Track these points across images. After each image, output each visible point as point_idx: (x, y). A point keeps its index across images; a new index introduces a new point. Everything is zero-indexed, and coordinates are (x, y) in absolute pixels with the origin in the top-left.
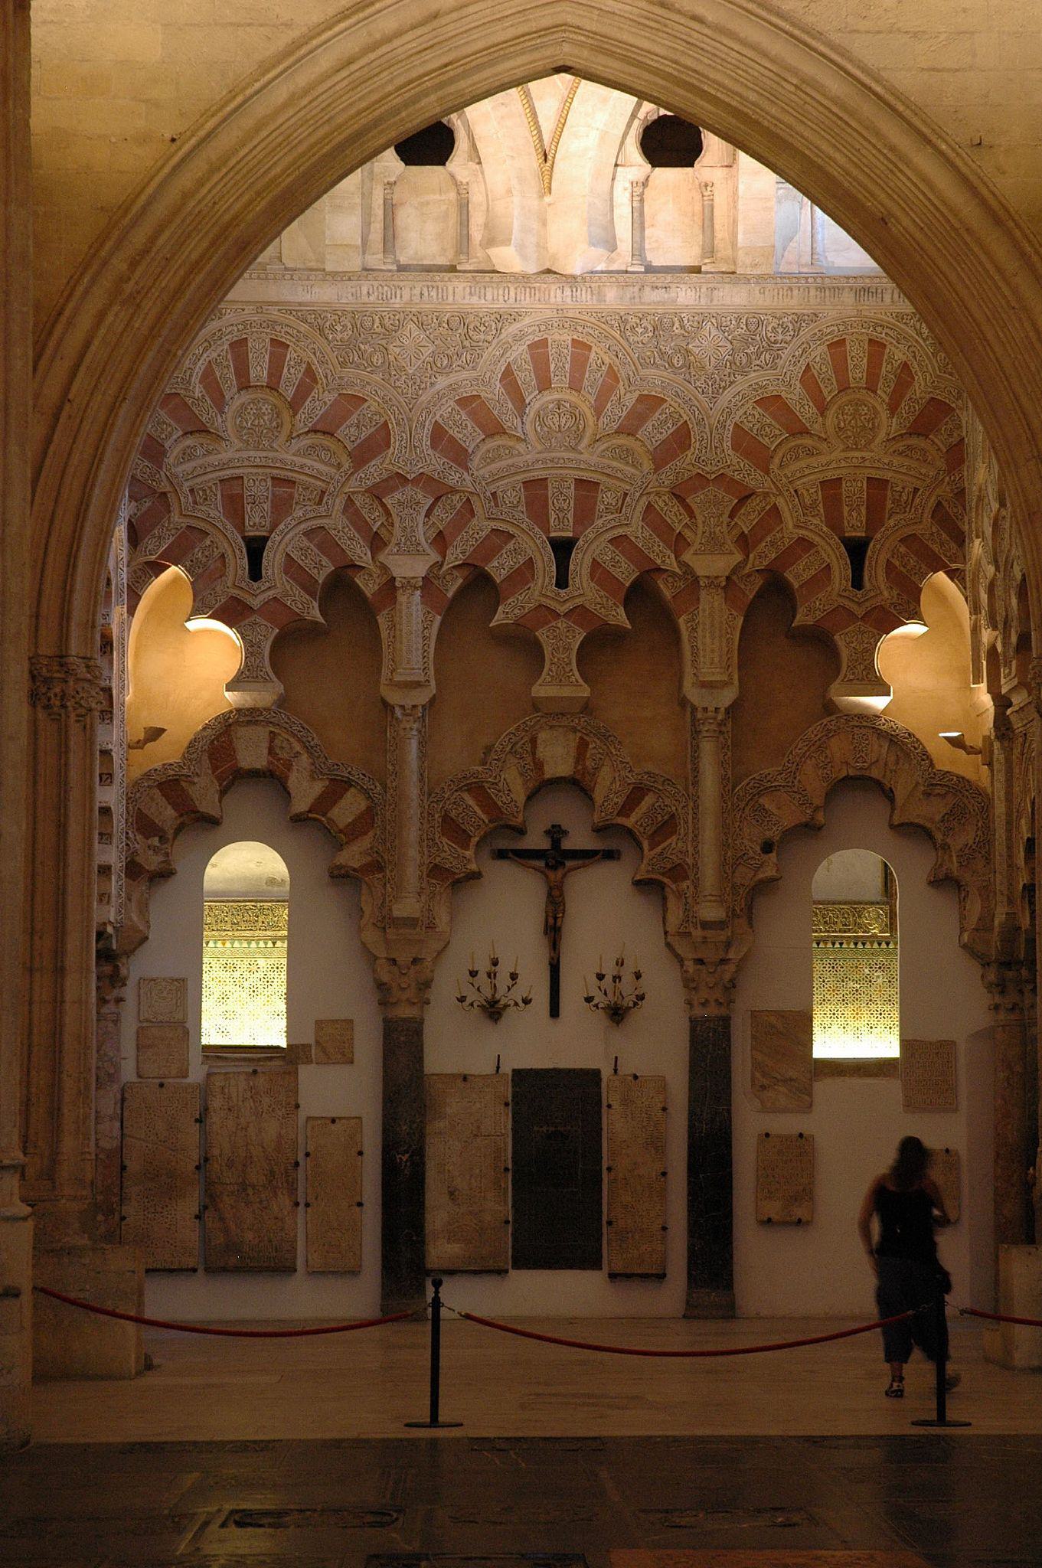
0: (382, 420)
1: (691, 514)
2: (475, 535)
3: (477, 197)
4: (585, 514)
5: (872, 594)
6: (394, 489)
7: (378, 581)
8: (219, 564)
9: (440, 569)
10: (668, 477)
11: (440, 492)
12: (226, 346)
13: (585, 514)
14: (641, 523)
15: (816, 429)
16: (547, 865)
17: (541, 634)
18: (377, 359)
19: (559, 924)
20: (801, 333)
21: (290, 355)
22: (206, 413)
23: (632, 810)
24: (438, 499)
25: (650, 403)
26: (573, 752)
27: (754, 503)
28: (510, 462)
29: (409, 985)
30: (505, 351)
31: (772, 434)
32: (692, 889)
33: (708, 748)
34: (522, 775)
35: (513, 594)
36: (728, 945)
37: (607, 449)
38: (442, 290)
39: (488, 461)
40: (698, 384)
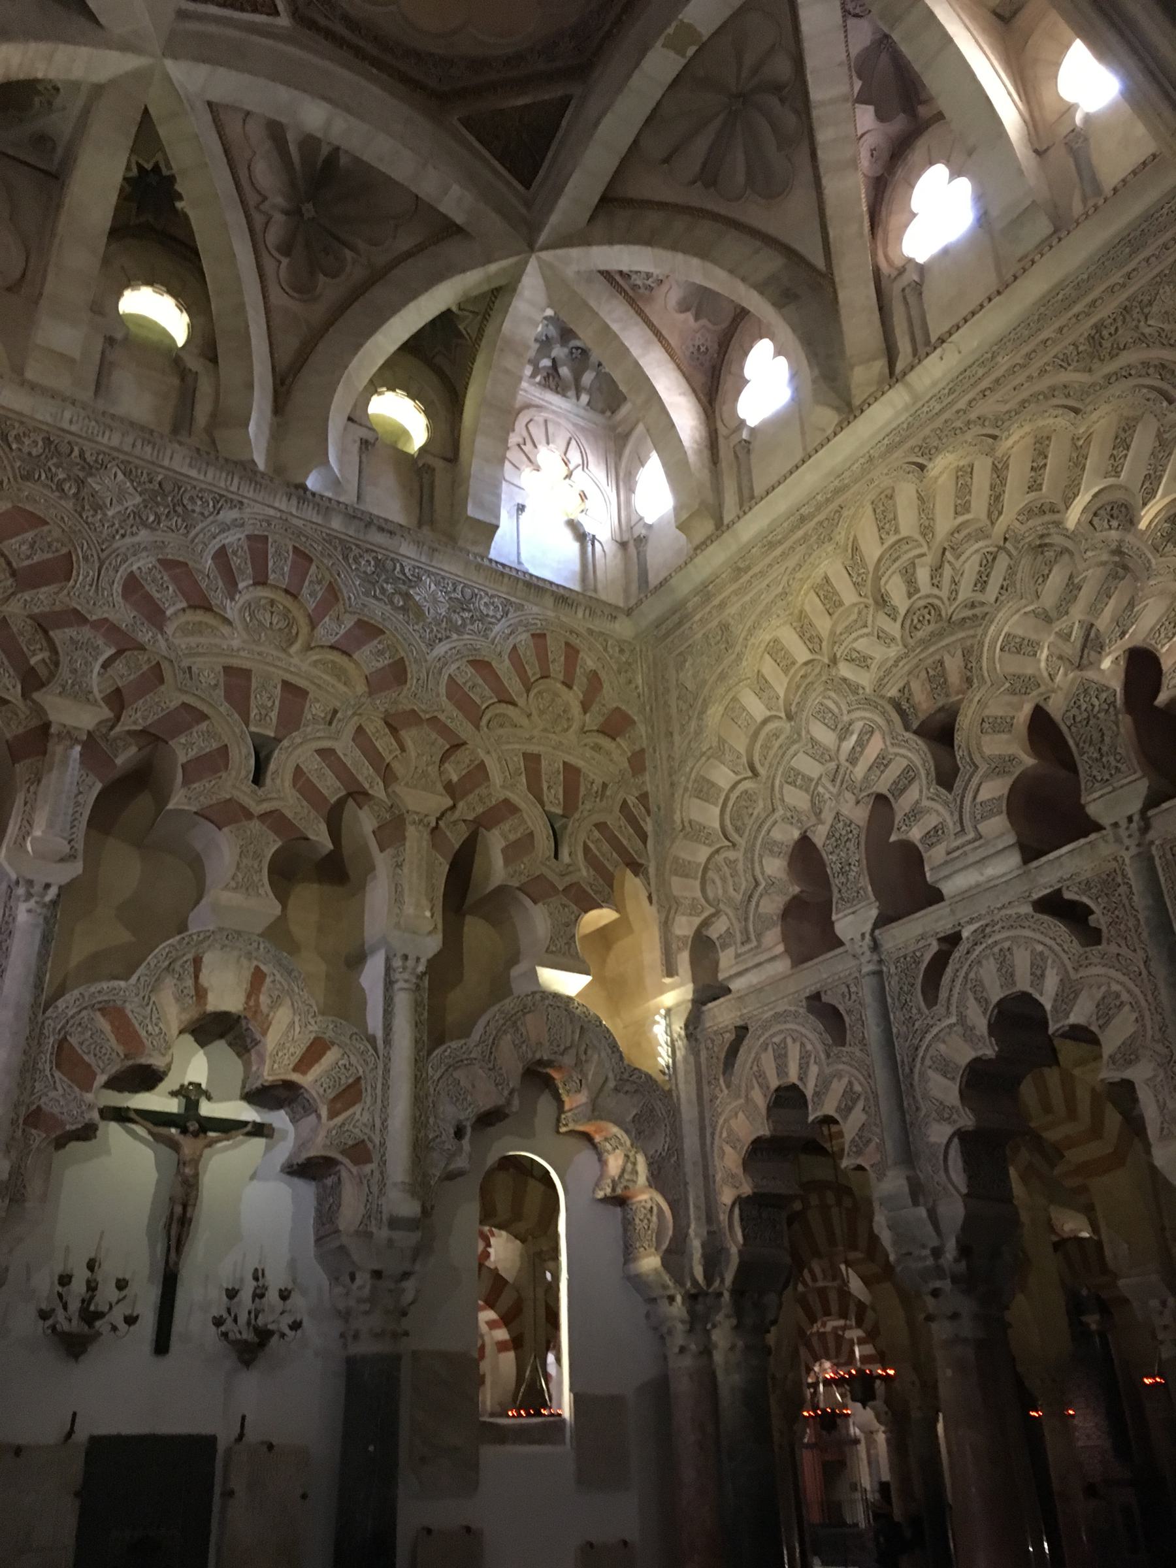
0: (64, 551)
1: (403, 749)
2: (162, 704)
3: (205, 387)
4: (291, 719)
5: (571, 868)
6: (71, 625)
11: (126, 645)
15: (521, 702)
16: (184, 1131)
23: (310, 1066)
24: (120, 653)
25: (368, 630)
26: (245, 985)
27: (462, 755)
30: (222, 531)
32: (377, 1174)
34: (177, 1000)
39: (185, 630)
40: (416, 627)
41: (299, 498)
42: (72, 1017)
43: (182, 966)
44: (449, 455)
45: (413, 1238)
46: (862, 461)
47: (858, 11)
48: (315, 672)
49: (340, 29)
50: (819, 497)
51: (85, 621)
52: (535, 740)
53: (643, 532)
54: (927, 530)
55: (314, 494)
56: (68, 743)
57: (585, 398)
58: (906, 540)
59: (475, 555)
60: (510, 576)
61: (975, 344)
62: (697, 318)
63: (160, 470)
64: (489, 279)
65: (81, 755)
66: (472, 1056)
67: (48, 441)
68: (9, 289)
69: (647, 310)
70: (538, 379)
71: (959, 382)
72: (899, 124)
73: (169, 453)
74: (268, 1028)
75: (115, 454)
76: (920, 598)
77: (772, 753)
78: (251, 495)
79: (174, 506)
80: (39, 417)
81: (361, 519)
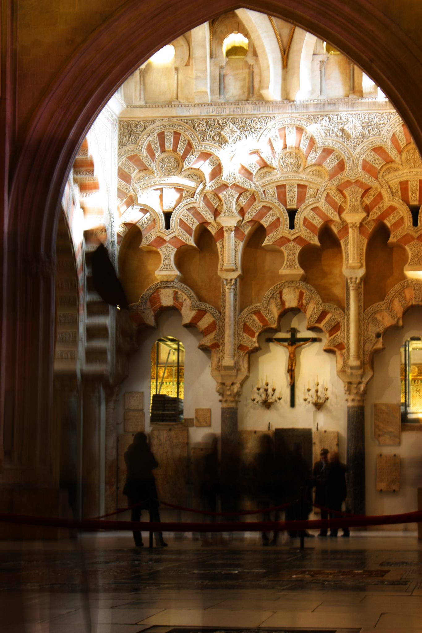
1: (345, 197)
3: (256, 71)
4: (301, 198)
6: (224, 190)
7: (217, 228)
8: (153, 223)
9: (242, 223)
10: (335, 182)
11: (242, 191)
12: (156, 135)
13: (301, 198)
14: (324, 201)
15: (397, 160)
17: (283, 249)
18: (216, 138)
19: (293, 368)
20: (391, 121)
21: (181, 137)
22: (148, 162)
25: (328, 151)
26: (297, 298)
28: (270, 178)
29: (230, 395)
31: (378, 162)
32: (346, 353)
33: (352, 294)
34: (276, 307)
35: (271, 232)
36: (362, 376)
37: (310, 171)
38: (242, 108)
42: (246, 317)
43: (276, 295)
45: (360, 372)
48: (309, 177)
51: (228, 187)
52: (405, 175)
56: (229, 232)
63: (245, 116)
65: (235, 234)
66: (381, 308)
67: (207, 123)
68: (186, 65)
73: (246, 108)
74: (306, 310)
75: (229, 117)
78: (277, 112)
79: (251, 129)
80: (202, 115)
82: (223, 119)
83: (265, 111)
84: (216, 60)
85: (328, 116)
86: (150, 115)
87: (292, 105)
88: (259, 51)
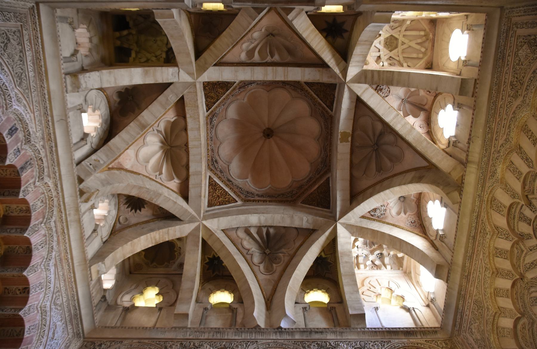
3: (240, 311)
20: (385, 347)
41: (280, 332)
44: (339, 301)
46: (477, 199)
47: (386, 95)
49: (257, 198)
50: (473, 225)
53: (432, 296)
54: (514, 195)
55: (285, 329)
57: (389, 267)
58: (511, 206)
59: (361, 329)
60: (379, 332)
61: (481, 130)
62: (405, 214)
64: (328, 238)
68: (171, 306)
69: (387, 221)
70: (368, 268)
71: (487, 145)
72: (422, 115)
73: (226, 334)
76: (534, 222)
77: (528, 338)
78: (260, 338)
81: (307, 331)
82: (200, 342)
83: (247, 337)
84: (201, 304)
85: (316, 342)
86: (119, 336)
87: (276, 332)
88: (243, 296)
